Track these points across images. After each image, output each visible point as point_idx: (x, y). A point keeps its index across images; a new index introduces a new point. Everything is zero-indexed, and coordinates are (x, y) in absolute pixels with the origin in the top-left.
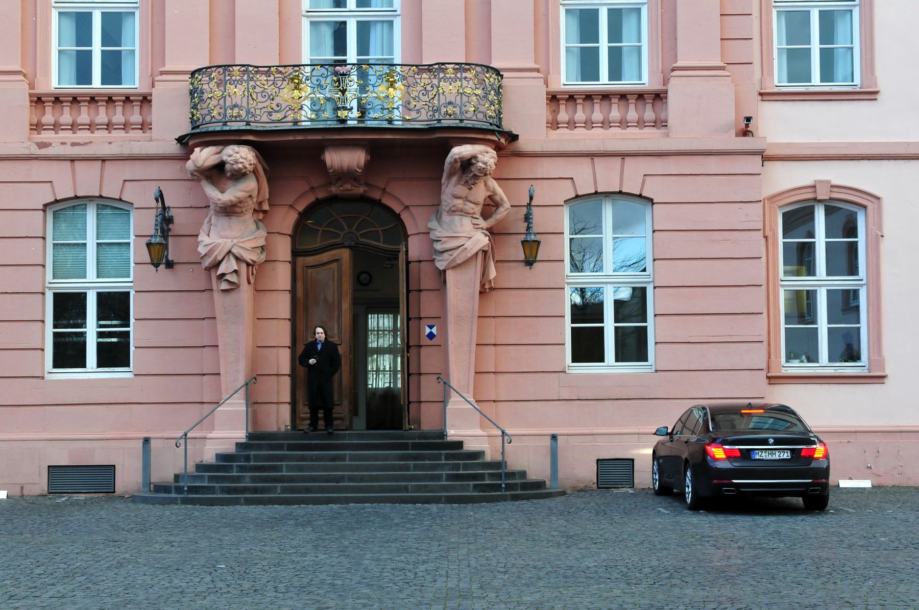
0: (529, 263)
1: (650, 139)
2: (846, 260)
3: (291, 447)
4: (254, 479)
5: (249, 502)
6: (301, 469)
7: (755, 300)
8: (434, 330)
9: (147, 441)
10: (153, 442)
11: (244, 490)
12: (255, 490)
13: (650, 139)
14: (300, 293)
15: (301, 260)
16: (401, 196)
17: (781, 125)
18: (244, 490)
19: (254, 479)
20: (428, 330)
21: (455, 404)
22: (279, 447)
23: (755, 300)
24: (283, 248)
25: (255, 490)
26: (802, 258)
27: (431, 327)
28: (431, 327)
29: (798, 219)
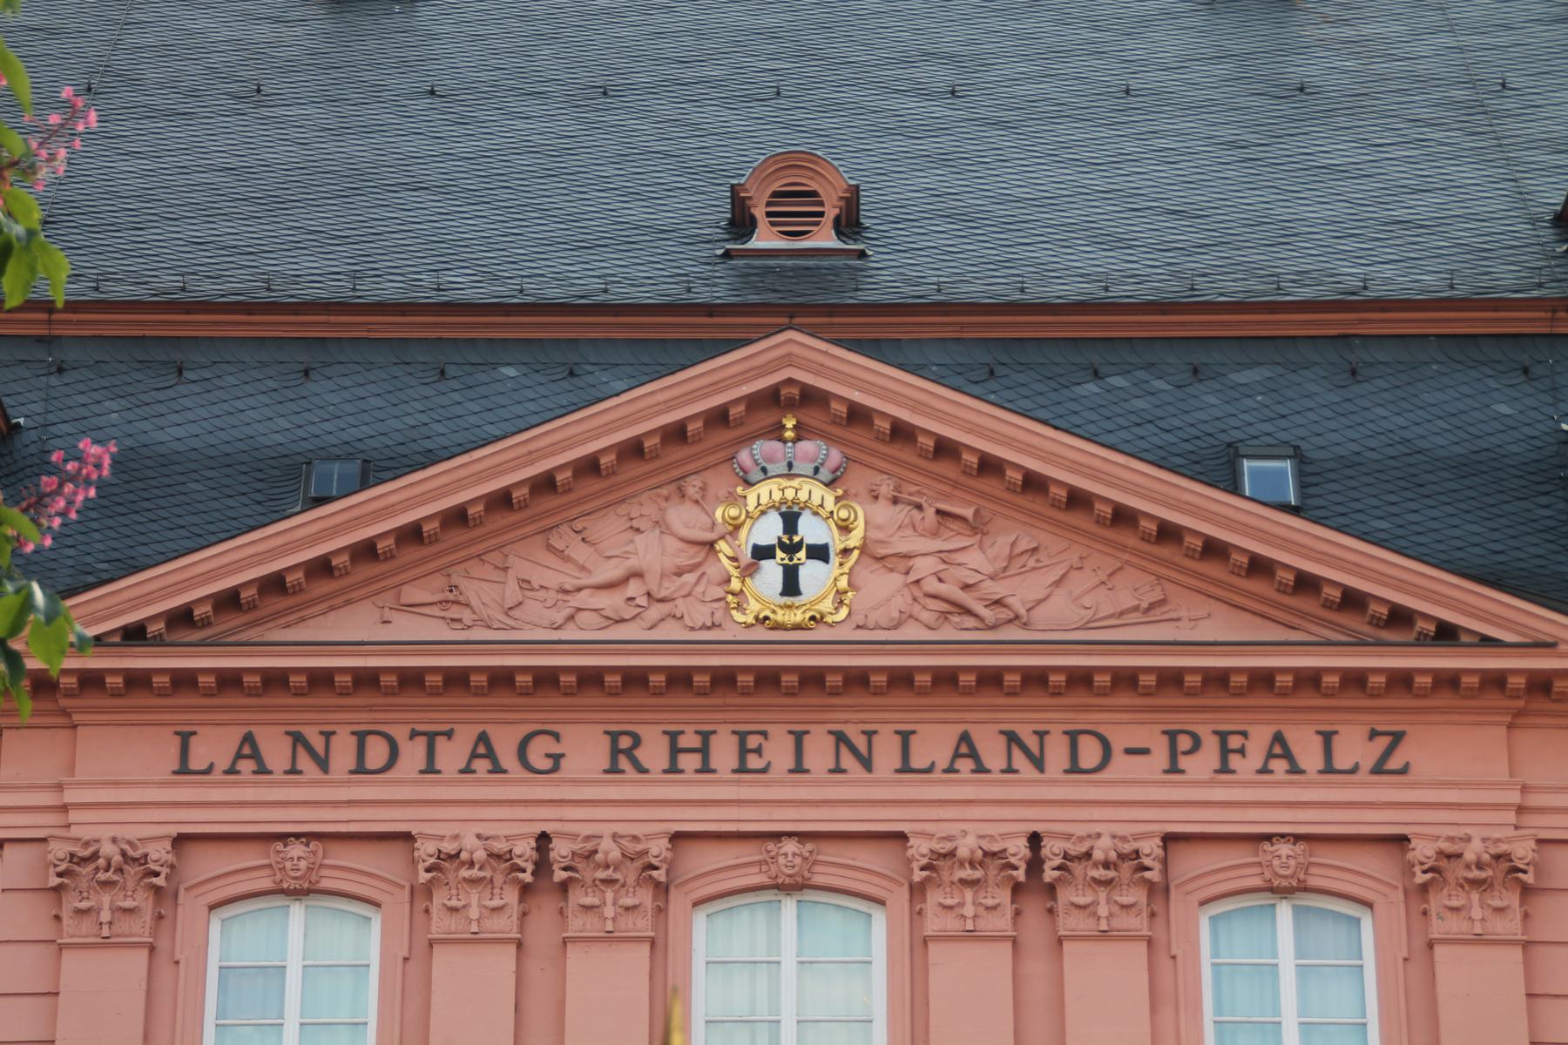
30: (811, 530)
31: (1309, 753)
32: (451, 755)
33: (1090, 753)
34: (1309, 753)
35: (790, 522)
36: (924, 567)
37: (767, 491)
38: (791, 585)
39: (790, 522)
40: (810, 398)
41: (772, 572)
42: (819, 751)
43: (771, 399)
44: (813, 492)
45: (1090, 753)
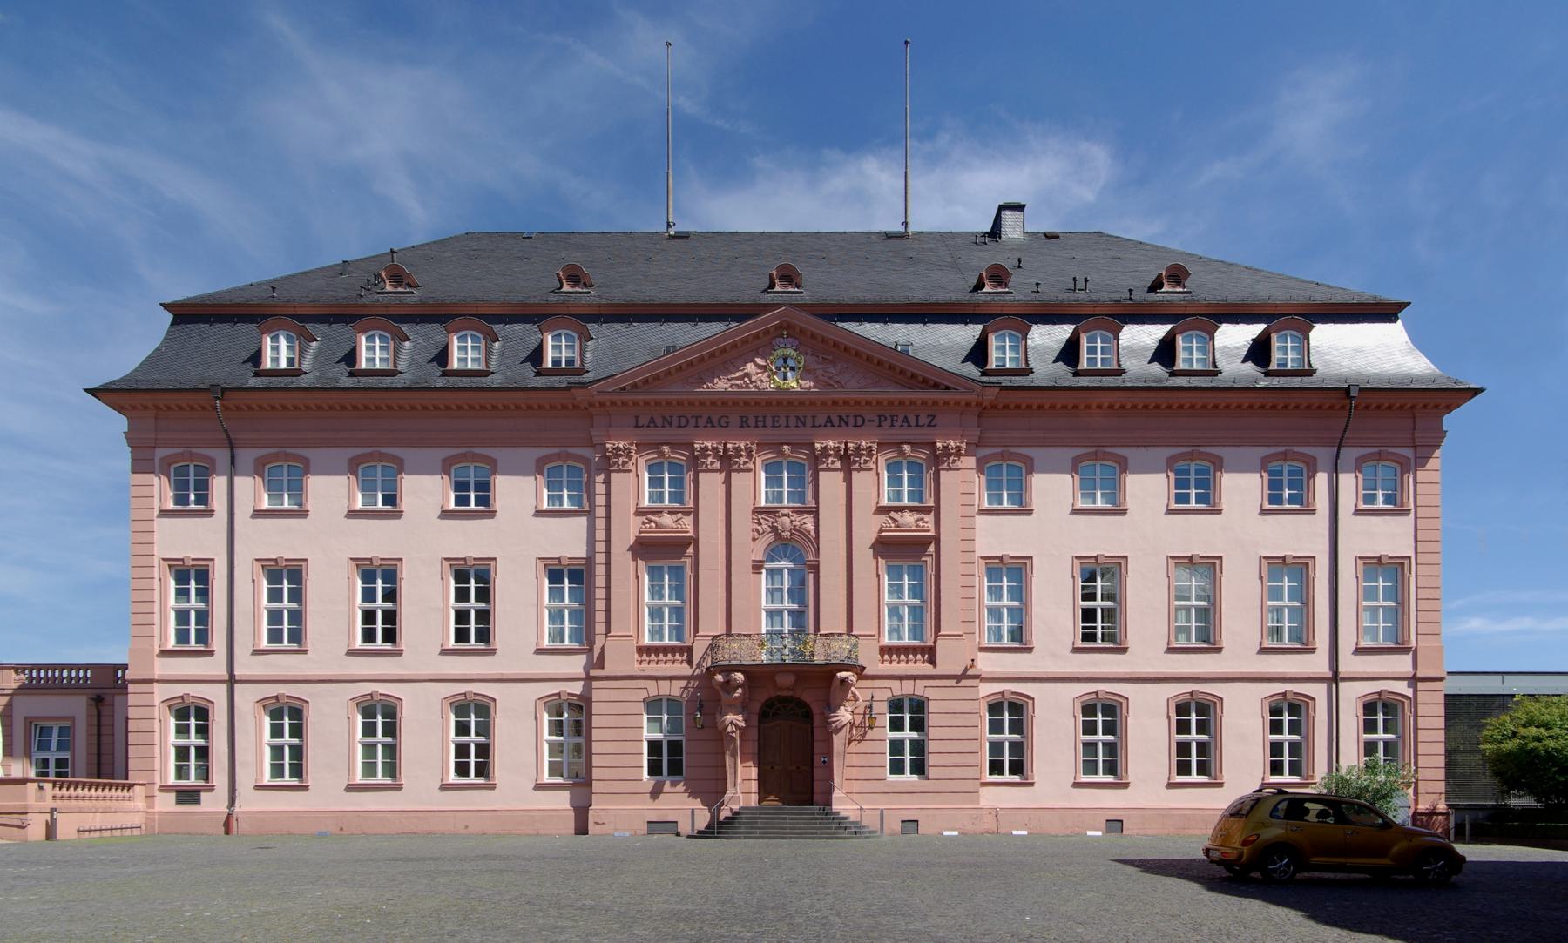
0: (871, 727)
1: (927, 669)
2: (1016, 727)
7: (973, 746)
13: (927, 669)
17: (987, 664)
21: (837, 794)
23: (973, 746)
24: (755, 720)
26: (996, 727)
29: (995, 708)
30: (791, 363)
31: (913, 421)
32: (702, 422)
33: (860, 421)
34: (913, 421)
35: (785, 360)
36: (819, 372)
37: (780, 352)
38: (785, 378)
39: (785, 360)
40: (789, 327)
41: (781, 374)
42: (792, 421)
43: (780, 327)
44: (790, 352)
45: (860, 421)
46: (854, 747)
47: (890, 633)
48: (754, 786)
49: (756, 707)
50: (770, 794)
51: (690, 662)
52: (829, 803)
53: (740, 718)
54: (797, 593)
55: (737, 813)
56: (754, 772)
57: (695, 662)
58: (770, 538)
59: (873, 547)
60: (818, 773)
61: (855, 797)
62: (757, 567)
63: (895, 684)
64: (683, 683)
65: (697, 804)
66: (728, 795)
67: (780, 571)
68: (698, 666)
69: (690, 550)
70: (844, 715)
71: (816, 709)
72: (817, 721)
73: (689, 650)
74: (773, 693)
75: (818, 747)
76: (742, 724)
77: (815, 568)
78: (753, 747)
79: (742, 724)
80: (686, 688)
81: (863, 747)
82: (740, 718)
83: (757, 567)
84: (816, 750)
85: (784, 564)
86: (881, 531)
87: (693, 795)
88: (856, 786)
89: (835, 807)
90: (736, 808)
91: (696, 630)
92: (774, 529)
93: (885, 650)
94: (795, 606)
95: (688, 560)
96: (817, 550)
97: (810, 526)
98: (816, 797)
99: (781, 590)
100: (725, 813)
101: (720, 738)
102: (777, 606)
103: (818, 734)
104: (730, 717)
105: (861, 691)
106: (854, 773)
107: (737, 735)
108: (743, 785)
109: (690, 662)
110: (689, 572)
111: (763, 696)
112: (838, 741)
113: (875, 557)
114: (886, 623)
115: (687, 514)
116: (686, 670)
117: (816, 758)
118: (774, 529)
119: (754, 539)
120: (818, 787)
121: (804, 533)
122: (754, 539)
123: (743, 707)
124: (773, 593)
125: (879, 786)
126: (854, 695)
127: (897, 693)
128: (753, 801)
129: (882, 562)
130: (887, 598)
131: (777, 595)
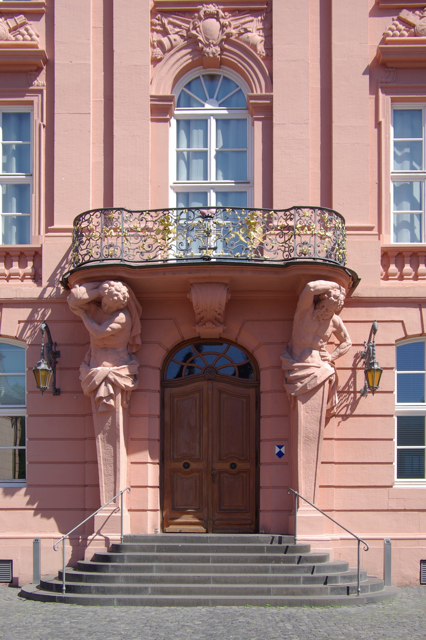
3: (160, 549)
4: (127, 580)
5: (122, 603)
6: (169, 570)
8: (283, 450)
9: (36, 541)
10: (43, 543)
11: (119, 590)
12: (128, 591)
14: (167, 418)
15: (168, 391)
16: (253, 336)
18: (119, 590)
19: (127, 580)
20: (277, 450)
22: (151, 549)
24: (154, 381)
25: (128, 591)
27: (280, 447)
28: (280, 447)
46: (334, 428)
47: (397, 230)
48: (153, 498)
49: (156, 356)
50: (184, 512)
51: (36, 277)
52: (288, 528)
53: (124, 371)
54: (232, 159)
55: (116, 548)
56: (152, 473)
57: (46, 275)
58: (182, 58)
59: (369, 71)
60: (268, 476)
61: (335, 516)
62: (161, 110)
63: (410, 315)
64: (24, 313)
65: (48, 530)
66: (100, 515)
67: (203, 122)
68: (51, 282)
69: (41, 81)
70: (319, 366)
71: (264, 359)
72: (267, 381)
73: (36, 255)
74: (188, 332)
75: (268, 429)
76: (129, 383)
77: (265, 112)
78: (151, 428)
79: (129, 383)
80: (29, 321)
81: (350, 428)
82: (124, 371)
83: (161, 110)
84: (264, 434)
85: (210, 109)
86: (383, 41)
87: (43, 511)
88: (338, 499)
89: (302, 536)
90: (115, 537)
91: (50, 220)
92: (191, 41)
93: (390, 256)
94: (230, 183)
95: (36, 99)
96: (270, 80)
97: (256, 37)
98: (265, 518)
99: (204, 155)
100: (95, 547)
101: (88, 412)
102: (197, 181)
103: (268, 404)
104: (105, 369)
105: (351, 326)
106: (332, 475)
107: (118, 404)
108: (132, 493)
109: (36, 277)
110: (38, 119)
111: (169, 334)
112: (307, 414)
113: (373, 91)
114: (391, 211)
115: (33, 16)
116: (30, 290)
117: (264, 447)
118: (191, 41)
119: (155, 61)
120: (268, 500)
121: (247, 50)
122: (155, 61)
123: (132, 352)
124: (186, 159)
125: (379, 498)
126: (338, 332)
127: (414, 329)
128: (151, 523)
129: (385, 99)
130: (391, 166)
131: (197, 164)
